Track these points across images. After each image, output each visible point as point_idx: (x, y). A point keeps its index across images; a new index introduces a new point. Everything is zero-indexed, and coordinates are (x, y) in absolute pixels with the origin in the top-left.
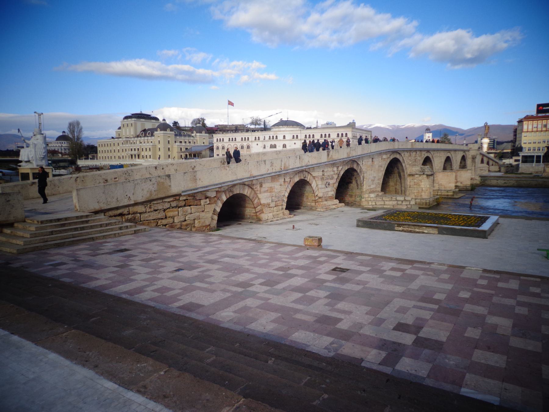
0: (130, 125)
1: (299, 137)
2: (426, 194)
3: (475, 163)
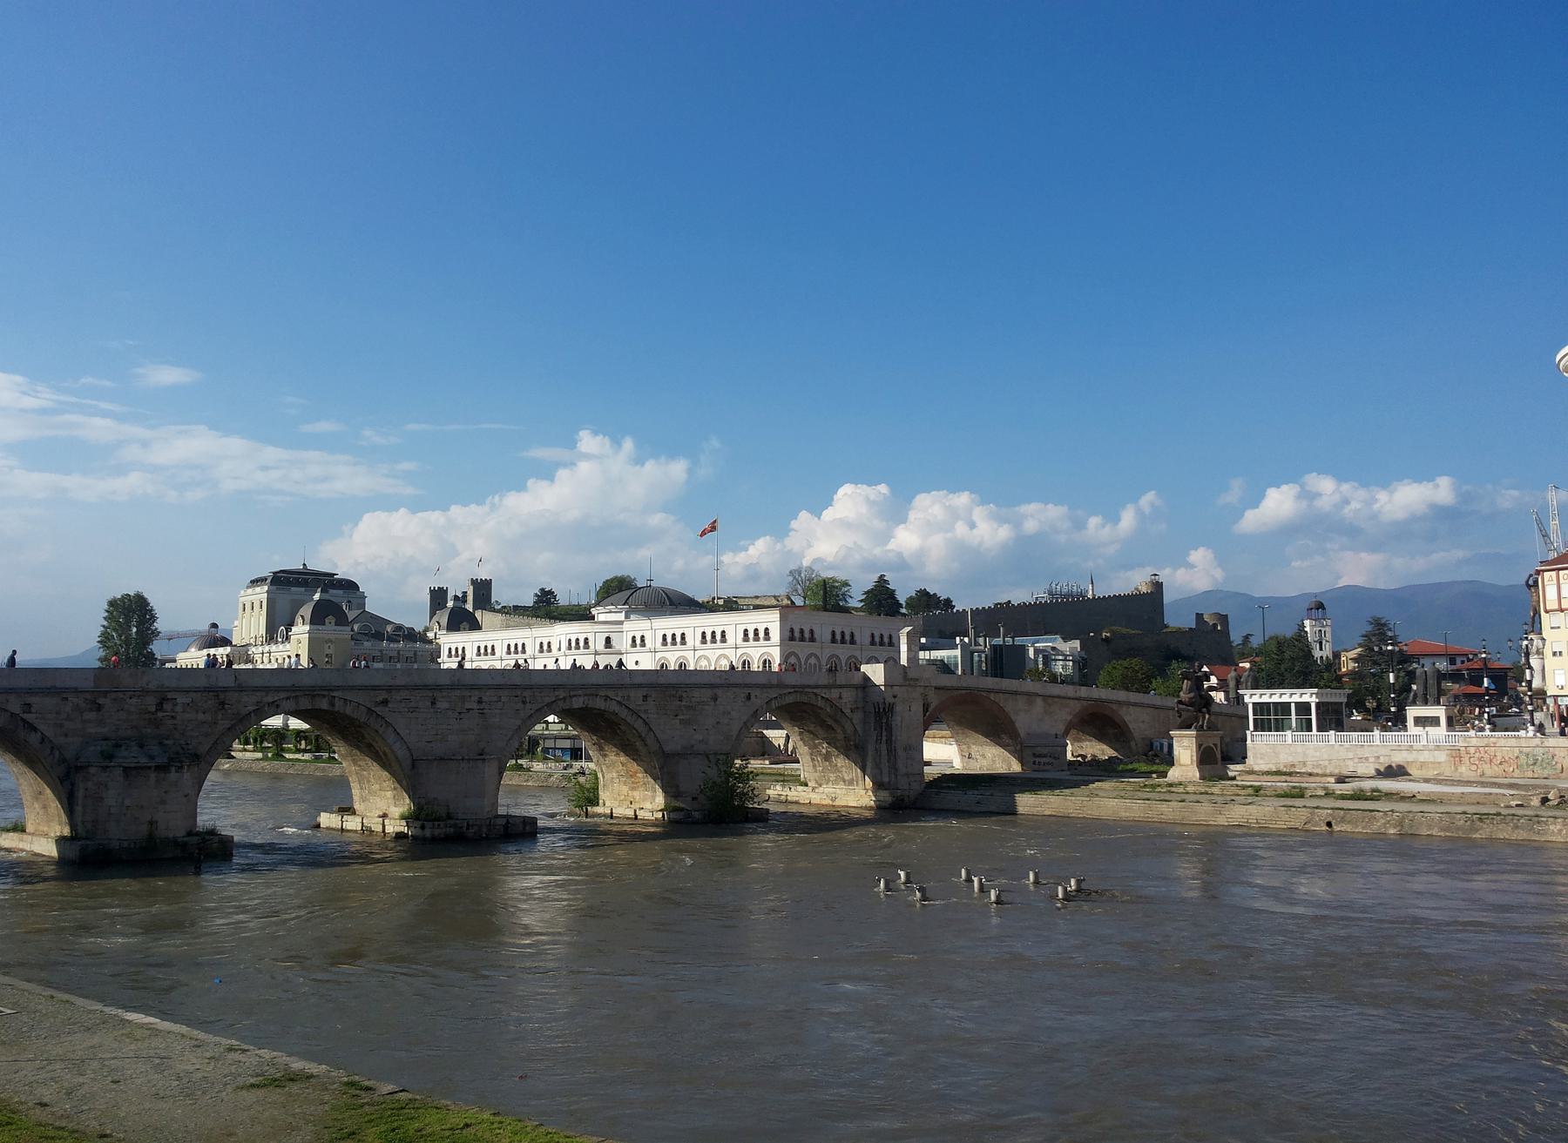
0: (257, 606)
3: (890, 729)
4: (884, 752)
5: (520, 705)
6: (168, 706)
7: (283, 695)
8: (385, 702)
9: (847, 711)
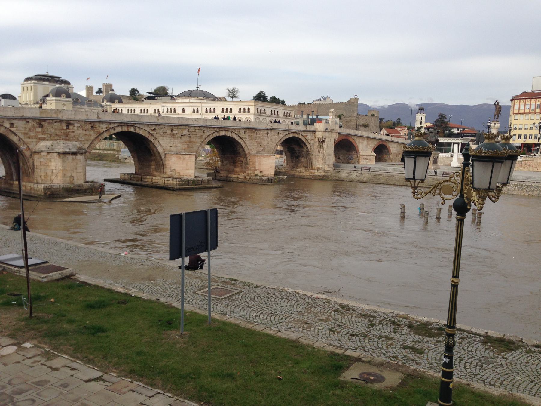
1: (200, 112)
2: (59, 178)
4: (321, 156)
5: (202, 134)
6: (71, 127)
7: (116, 125)
8: (154, 130)
9: (309, 140)
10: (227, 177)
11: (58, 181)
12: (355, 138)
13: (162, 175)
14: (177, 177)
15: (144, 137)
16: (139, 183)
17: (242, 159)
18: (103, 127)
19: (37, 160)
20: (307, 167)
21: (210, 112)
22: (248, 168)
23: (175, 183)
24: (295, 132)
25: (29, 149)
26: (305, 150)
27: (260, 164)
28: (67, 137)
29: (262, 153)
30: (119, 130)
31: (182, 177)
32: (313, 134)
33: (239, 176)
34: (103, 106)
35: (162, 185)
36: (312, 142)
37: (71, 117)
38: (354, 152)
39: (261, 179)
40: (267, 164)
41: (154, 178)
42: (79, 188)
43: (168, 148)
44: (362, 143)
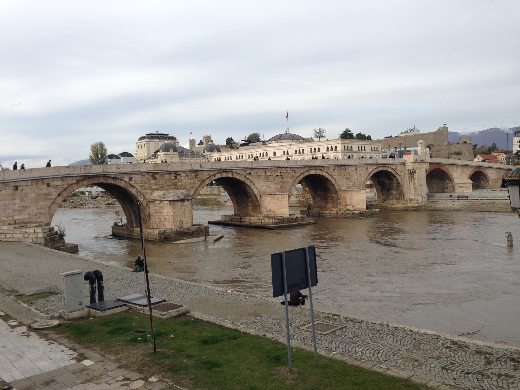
0: (143, 146)
1: (290, 154)
2: (170, 222)
4: (412, 187)
5: (293, 174)
6: (178, 177)
7: (216, 172)
8: (249, 174)
9: (399, 173)
10: (320, 213)
11: (169, 226)
12: (448, 167)
13: (259, 215)
14: (272, 216)
15: (241, 181)
16: (239, 223)
17: (333, 195)
18: (206, 175)
19: (153, 208)
20: (399, 199)
21: (300, 153)
22: (340, 204)
23: (271, 221)
24: (384, 166)
25: (145, 199)
26: (395, 182)
27: (351, 199)
28: (176, 186)
29: (353, 188)
30: (219, 176)
31: (277, 215)
32: (403, 166)
33: (331, 212)
34: (204, 156)
35: (259, 224)
36: (402, 174)
37: (179, 169)
38: (448, 181)
39: (353, 213)
40: (359, 198)
41: (252, 218)
42: (187, 231)
43: (263, 189)
44: (456, 171)
